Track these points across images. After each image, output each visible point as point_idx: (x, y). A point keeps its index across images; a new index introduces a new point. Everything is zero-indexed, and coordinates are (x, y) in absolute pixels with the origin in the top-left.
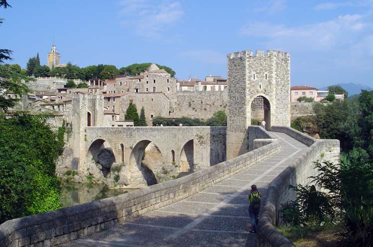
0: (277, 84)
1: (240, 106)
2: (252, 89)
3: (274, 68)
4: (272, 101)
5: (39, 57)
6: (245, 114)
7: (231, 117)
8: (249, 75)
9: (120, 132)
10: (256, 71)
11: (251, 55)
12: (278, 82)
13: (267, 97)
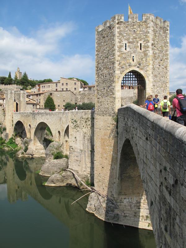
0: (155, 57)
1: (108, 85)
2: (123, 62)
3: (151, 36)
4: (148, 77)
5: (11, 73)
6: (113, 94)
7: (98, 98)
8: (119, 44)
9: (29, 116)
10: (128, 39)
11: (121, 20)
12: (156, 54)
13: (142, 72)
